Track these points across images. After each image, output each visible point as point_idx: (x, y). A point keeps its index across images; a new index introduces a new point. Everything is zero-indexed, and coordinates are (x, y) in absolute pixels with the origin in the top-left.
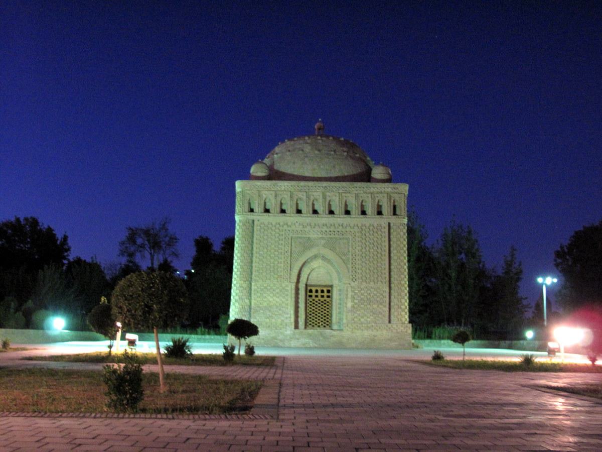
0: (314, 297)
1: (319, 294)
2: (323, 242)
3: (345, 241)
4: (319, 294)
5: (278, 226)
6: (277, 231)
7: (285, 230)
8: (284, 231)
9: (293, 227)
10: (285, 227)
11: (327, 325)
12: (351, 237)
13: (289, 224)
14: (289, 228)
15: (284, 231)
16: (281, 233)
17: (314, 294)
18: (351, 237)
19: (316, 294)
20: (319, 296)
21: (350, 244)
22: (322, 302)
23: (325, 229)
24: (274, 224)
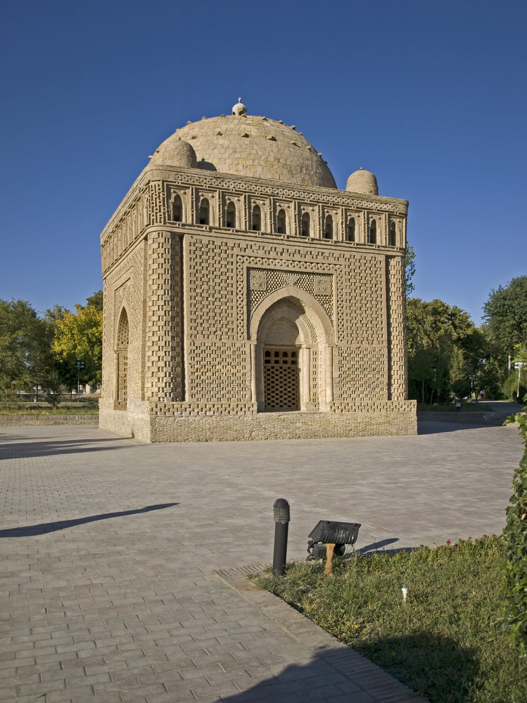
0: (272, 364)
1: (281, 359)
2: (294, 278)
3: (327, 278)
4: (281, 359)
5: (224, 248)
6: (223, 255)
7: (237, 255)
8: (235, 256)
9: (249, 252)
10: (236, 251)
11: (293, 404)
12: (334, 272)
13: (243, 245)
14: (242, 253)
15: (235, 256)
16: (230, 259)
17: (273, 359)
18: (334, 272)
19: (277, 359)
20: (281, 362)
21: (333, 284)
22: (285, 370)
23: (297, 257)
24: (218, 243)
